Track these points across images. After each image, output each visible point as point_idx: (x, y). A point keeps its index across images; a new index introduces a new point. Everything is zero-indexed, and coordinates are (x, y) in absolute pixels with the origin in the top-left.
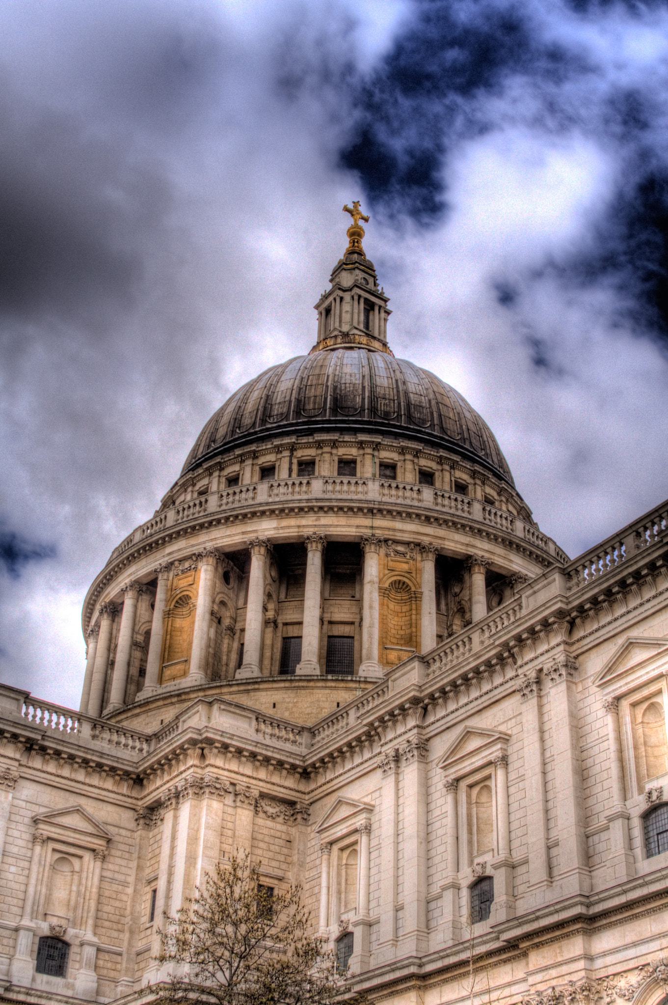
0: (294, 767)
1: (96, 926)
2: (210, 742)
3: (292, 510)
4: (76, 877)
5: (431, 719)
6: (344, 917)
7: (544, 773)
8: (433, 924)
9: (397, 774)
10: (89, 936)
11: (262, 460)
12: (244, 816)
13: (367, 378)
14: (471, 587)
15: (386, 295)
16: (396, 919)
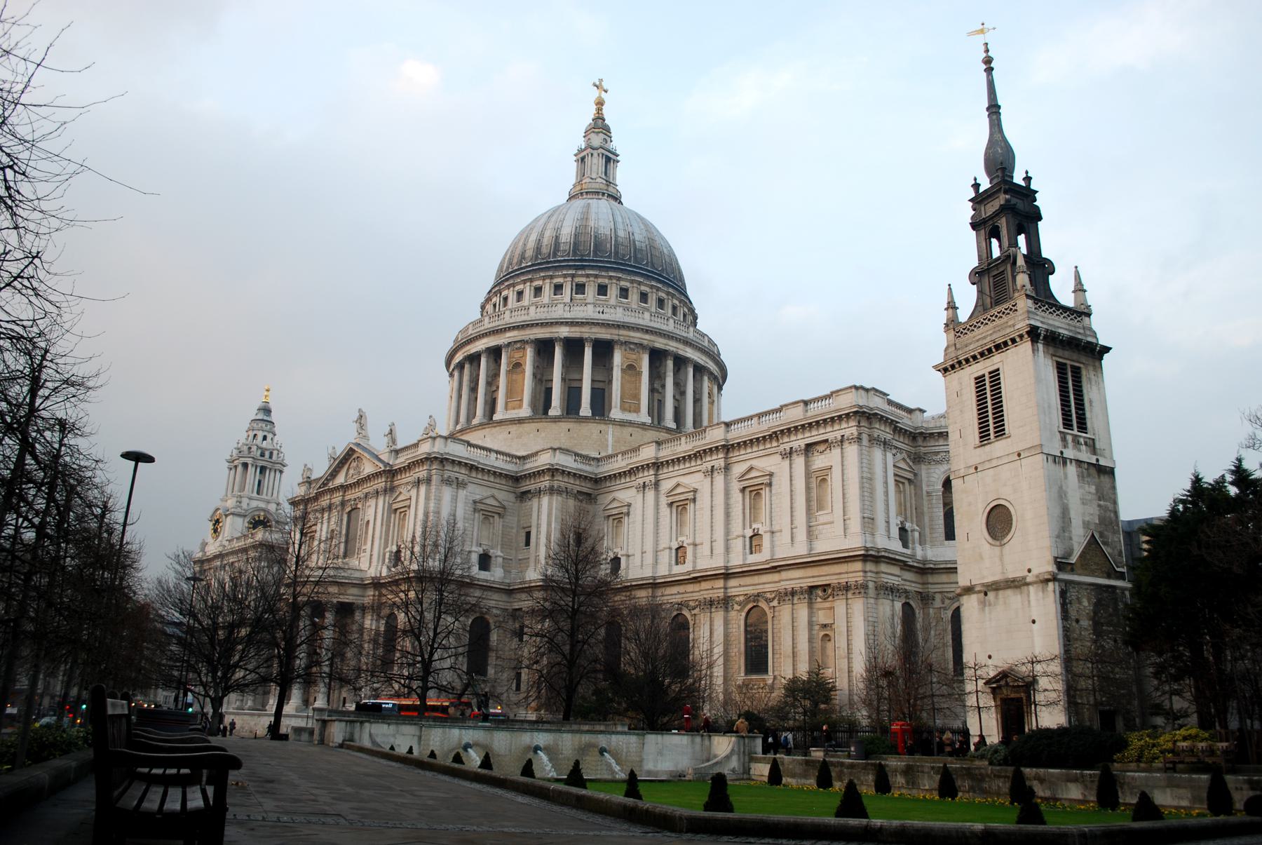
0: (591, 478)
1: (502, 548)
2: (557, 469)
3: (578, 322)
4: (492, 526)
5: (661, 472)
6: (615, 550)
7: (712, 511)
8: (659, 561)
9: (644, 493)
10: (499, 553)
11: (556, 281)
12: (571, 503)
13: (613, 230)
14: (666, 366)
15: (618, 152)
16: (642, 557)
